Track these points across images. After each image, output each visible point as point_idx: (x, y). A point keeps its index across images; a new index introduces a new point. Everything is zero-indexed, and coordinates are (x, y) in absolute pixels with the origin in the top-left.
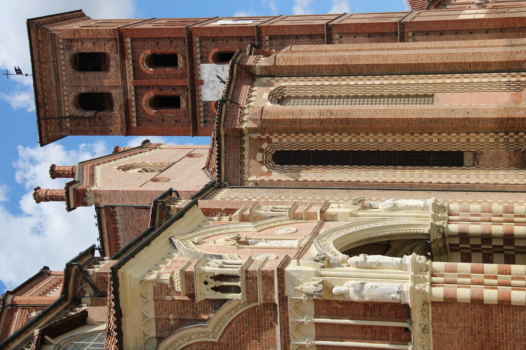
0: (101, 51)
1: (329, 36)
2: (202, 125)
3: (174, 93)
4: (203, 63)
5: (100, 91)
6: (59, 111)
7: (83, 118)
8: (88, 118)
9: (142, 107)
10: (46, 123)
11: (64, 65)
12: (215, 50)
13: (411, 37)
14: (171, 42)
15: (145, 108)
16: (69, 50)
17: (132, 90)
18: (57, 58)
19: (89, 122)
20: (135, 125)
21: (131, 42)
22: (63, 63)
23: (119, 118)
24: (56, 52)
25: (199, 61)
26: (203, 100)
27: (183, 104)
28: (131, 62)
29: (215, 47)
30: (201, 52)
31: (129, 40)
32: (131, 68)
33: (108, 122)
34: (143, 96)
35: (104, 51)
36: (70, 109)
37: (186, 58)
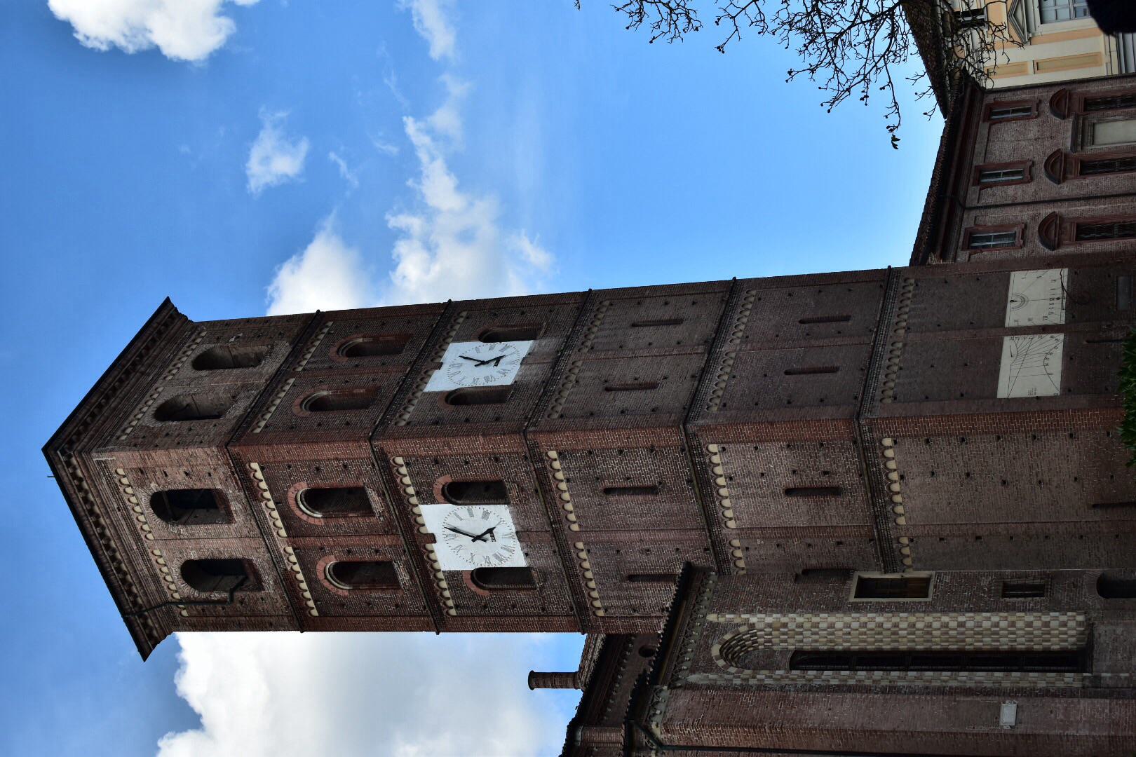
0: (207, 487)
1: (696, 449)
2: (453, 612)
3: (377, 557)
4: (423, 503)
5: (227, 556)
6: (160, 590)
7: (207, 601)
8: (219, 602)
9: (317, 581)
10: (141, 616)
11: (142, 514)
12: (442, 481)
13: (891, 447)
14: (345, 466)
15: (326, 584)
16: (142, 487)
17: (290, 554)
18: (124, 503)
19: (223, 608)
20: (315, 612)
21: (262, 469)
22: (138, 509)
23: (280, 601)
24: (118, 493)
25: (414, 500)
26: (443, 569)
27: (404, 577)
28: (271, 504)
29: (442, 474)
30: (414, 484)
31: (255, 466)
32: (276, 514)
33: (260, 608)
34: (314, 564)
35: (212, 487)
36: (180, 588)
37: (384, 494)
